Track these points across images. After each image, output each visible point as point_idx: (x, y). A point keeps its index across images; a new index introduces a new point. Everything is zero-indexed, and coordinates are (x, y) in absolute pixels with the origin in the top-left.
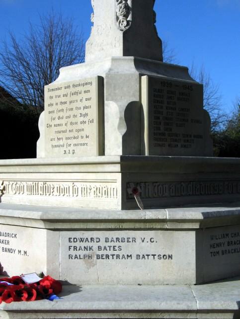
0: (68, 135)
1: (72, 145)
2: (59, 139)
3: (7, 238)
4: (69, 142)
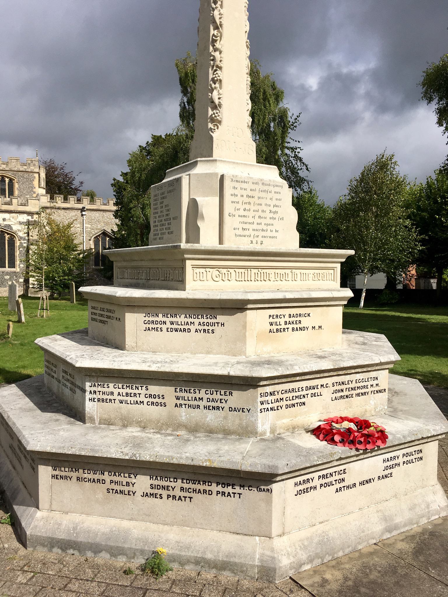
0: (255, 226)
1: (260, 237)
2: (244, 229)
3: (298, 319)
4: (257, 233)
